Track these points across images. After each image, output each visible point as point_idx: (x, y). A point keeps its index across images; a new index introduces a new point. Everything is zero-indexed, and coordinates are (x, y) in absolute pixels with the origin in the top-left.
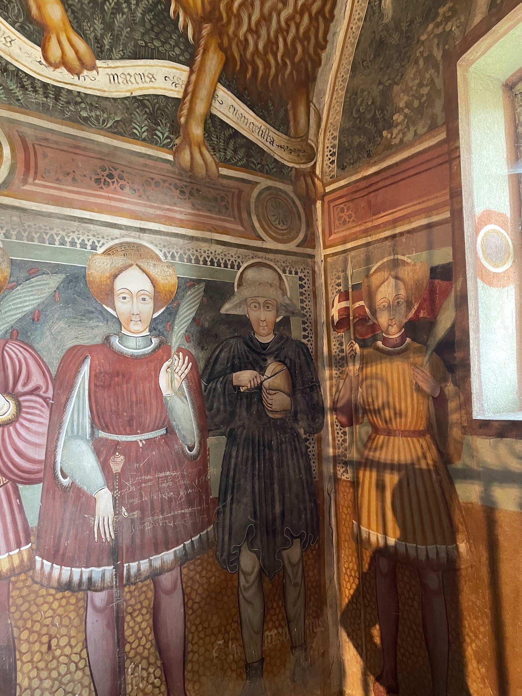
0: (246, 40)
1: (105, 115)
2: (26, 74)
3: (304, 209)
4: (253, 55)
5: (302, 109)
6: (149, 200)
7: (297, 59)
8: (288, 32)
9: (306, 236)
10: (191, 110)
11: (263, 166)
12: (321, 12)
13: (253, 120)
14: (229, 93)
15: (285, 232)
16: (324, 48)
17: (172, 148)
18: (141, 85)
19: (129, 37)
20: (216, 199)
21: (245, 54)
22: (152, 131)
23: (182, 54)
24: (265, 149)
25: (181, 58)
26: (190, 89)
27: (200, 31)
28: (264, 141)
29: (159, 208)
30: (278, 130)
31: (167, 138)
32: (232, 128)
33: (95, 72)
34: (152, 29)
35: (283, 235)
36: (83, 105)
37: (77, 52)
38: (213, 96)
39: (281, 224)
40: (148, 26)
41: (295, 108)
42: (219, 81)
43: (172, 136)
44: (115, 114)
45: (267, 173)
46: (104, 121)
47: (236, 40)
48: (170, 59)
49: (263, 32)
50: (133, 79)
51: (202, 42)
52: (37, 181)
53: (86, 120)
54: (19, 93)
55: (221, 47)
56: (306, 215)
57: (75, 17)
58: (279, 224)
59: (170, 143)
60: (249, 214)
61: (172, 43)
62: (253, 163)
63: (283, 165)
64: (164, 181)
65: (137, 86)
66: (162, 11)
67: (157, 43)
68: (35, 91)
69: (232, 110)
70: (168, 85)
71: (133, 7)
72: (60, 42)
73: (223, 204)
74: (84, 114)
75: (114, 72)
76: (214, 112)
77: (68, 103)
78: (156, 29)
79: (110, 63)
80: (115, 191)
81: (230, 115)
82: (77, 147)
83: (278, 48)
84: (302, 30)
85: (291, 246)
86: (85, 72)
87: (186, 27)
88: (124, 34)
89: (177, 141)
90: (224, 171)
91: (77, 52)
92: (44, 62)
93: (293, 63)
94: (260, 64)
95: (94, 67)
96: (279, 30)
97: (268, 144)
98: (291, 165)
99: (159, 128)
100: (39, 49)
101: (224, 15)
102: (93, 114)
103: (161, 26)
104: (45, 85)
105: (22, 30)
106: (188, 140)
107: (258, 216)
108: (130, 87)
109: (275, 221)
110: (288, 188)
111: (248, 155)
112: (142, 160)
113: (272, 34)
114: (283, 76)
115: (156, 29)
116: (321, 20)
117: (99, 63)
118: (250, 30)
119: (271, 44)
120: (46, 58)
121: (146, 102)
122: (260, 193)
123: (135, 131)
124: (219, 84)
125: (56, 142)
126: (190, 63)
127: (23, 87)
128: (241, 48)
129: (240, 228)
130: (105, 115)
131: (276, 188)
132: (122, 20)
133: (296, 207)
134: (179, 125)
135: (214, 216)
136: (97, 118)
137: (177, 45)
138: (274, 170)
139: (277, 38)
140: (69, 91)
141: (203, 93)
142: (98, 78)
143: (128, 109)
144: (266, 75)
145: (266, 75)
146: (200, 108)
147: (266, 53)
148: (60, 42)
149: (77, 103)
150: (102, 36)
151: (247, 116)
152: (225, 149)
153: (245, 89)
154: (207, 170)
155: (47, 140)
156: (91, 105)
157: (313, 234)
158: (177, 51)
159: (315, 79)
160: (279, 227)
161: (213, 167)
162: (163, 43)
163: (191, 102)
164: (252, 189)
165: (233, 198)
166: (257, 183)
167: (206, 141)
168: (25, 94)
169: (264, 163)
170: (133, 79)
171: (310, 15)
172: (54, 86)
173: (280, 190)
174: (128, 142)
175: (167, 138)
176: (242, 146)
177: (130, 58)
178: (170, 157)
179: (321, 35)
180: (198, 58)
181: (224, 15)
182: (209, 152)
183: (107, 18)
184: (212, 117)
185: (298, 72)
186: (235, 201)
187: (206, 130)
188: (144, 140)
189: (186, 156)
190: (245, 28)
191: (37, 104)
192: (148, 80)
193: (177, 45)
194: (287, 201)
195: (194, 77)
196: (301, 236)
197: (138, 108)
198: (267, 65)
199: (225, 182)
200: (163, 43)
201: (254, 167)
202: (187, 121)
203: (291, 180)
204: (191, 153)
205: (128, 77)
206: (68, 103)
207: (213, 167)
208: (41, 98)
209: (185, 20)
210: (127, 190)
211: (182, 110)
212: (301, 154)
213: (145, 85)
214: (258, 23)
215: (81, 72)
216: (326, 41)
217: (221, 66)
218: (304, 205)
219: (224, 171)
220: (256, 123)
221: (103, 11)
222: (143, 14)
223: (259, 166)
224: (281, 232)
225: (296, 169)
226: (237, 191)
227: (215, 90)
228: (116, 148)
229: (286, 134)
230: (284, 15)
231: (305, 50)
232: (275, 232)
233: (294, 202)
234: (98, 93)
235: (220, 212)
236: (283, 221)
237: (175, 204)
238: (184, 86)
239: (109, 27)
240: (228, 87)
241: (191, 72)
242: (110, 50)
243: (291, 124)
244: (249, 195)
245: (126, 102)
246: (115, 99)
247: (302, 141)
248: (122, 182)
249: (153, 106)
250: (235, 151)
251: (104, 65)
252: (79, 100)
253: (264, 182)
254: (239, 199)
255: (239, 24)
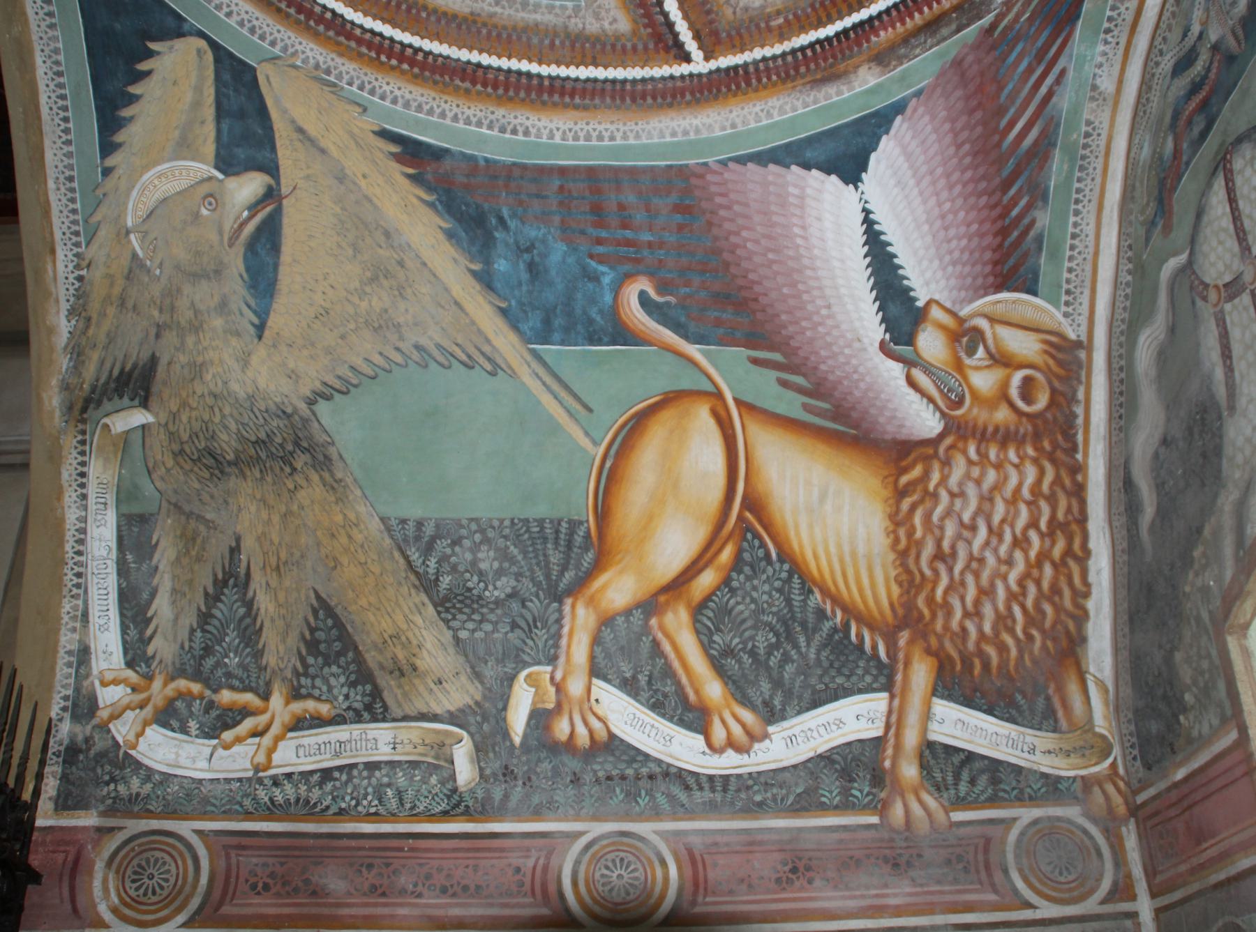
0: (964, 630)
1: (784, 791)
2: (690, 772)
3: (1108, 839)
4: (978, 643)
5: (1073, 688)
6: (847, 888)
7: (1048, 624)
8: (1024, 594)
9: (1115, 884)
10: (898, 747)
11: (1022, 791)
12: (1068, 552)
13: (996, 729)
14: (952, 705)
15: (1073, 885)
16: (1087, 595)
17: (876, 807)
18: (826, 737)
19: (805, 686)
20: (948, 862)
21: (966, 648)
22: (845, 792)
23: (876, 678)
24: (1022, 763)
25: (875, 686)
26: (894, 718)
27: (895, 644)
28: (1018, 753)
29: (863, 897)
30: (1040, 729)
31: (868, 795)
32: (963, 750)
33: (767, 741)
34: (831, 666)
35: (1070, 890)
36: (756, 788)
37: (743, 725)
38: (927, 716)
39: (1065, 873)
40: (826, 664)
41: (1060, 689)
42: (934, 693)
43: (874, 790)
44: (797, 784)
45: (1031, 798)
46: (782, 800)
47: (948, 635)
48: (860, 691)
49: (988, 610)
50: (815, 734)
51: (901, 655)
52: (708, 899)
53: (760, 804)
54: (682, 796)
55: (928, 652)
56: (1112, 847)
57: (738, 688)
58: (1061, 874)
59: (872, 800)
60: (1006, 871)
61: (860, 672)
62: (1004, 791)
63: (1059, 779)
64: (868, 856)
65: (820, 740)
66: (840, 642)
67: (839, 680)
68: (701, 788)
69: (959, 726)
70: (863, 723)
71: (804, 650)
72: (723, 722)
73: (960, 866)
74: (758, 798)
75: (790, 733)
76: (933, 737)
77: (738, 790)
78: (836, 665)
79: (785, 724)
80: (802, 889)
81: (958, 733)
82: (751, 843)
83: (1014, 621)
84: (1046, 585)
85: (1090, 906)
86: (756, 746)
87: (874, 647)
88: (797, 685)
89: (883, 795)
90: (958, 816)
91: (743, 725)
92: (707, 751)
93: (1043, 632)
94: (991, 651)
95: (766, 736)
96: (1012, 596)
97: (1026, 755)
98: (1071, 773)
99: (856, 785)
100: (701, 737)
101: (926, 612)
102: (769, 795)
103: (843, 658)
104: (711, 778)
105: (682, 723)
106: (898, 789)
107: (1021, 871)
108: (813, 743)
109: (1052, 872)
110: (1072, 812)
111: (995, 781)
112: (836, 836)
113: (1001, 606)
114: (1031, 653)
115: (836, 665)
116: (1071, 563)
117: (771, 729)
118: (966, 614)
119: (1005, 621)
120: (709, 744)
121: (836, 757)
122: (1022, 834)
123: (823, 799)
124: (935, 700)
125: (727, 844)
126: (888, 687)
127: (687, 788)
128: (959, 642)
129: (992, 897)
130: (784, 791)
131: (1049, 818)
132: (793, 670)
133: (1091, 838)
134: (883, 770)
135: (947, 888)
136: (774, 799)
137: (867, 672)
138: (1043, 790)
139: (1009, 608)
140: (739, 776)
141: (913, 718)
142: (771, 747)
143: (812, 773)
144: (1003, 663)
145: (1003, 663)
146: (911, 739)
147: (997, 633)
148: (723, 722)
149: (748, 788)
150: (771, 697)
151: (985, 726)
152: (956, 784)
153: (975, 690)
154: (931, 822)
155: (716, 844)
156: (766, 784)
157: (1129, 876)
158: (868, 679)
159: (1084, 640)
160: (1062, 879)
161: (940, 815)
162: (848, 677)
163: (898, 735)
164: (1008, 829)
165: (976, 853)
166: (1015, 819)
167: (926, 783)
168: (690, 796)
169: (1023, 784)
170: (815, 734)
171: (1054, 564)
172: (721, 776)
173: (1059, 819)
174: (816, 817)
175: (868, 795)
176: (982, 771)
177: (808, 709)
178: (875, 820)
179: (1077, 580)
180: (899, 677)
181: (926, 612)
182: (931, 795)
183: (775, 674)
184: (931, 745)
185: (1054, 640)
186: (981, 857)
187: (923, 766)
188: (836, 807)
189: (898, 811)
190: (958, 614)
191: (704, 803)
192: (834, 727)
193: (867, 672)
194: (1072, 832)
195: (896, 702)
196: (1106, 885)
197: (825, 767)
198: (1002, 648)
199: (962, 831)
200: (848, 677)
201: (1006, 796)
202: (894, 764)
203: (1076, 798)
204: (906, 805)
205: (809, 733)
206: (738, 790)
207: (940, 815)
208: (707, 795)
209: (873, 640)
210: (818, 883)
211: (884, 751)
212: (1087, 752)
213: (832, 735)
214: (977, 603)
215: (751, 747)
216: (1087, 584)
217: (933, 675)
218: (1106, 832)
219: (958, 816)
220: (1000, 731)
221: (768, 668)
222: (818, 652)
223: (1015, 792)
224: (1067, 886)
225: (1083, 777)
226: (981, 842)
227: (929, 708)
228: (800, 829)
229: (1054, 731)
230: (1013, 578)
231: (1058, 609)
232: (1054, 889)
233: (1085, 832)
234: (773, 766)
235: (956, 881)
236: (1067, 869)
237: (886, 886)
238: (884, 719)
239: (777, 683)
240: (950, 697)
241: (892, 697)
242: (783, 710)
243: (1060, 714)
244: (1003, 842)
245: (810, 765)
246: (795, 767)
247: (1086, 732)
248: (808, 874)
249: (845, 759)
250: (972, 782)
251: (779, 729)
252: (750, 782)
253: (1027, 814)
254: (986, 851)
255: (949, 613)
